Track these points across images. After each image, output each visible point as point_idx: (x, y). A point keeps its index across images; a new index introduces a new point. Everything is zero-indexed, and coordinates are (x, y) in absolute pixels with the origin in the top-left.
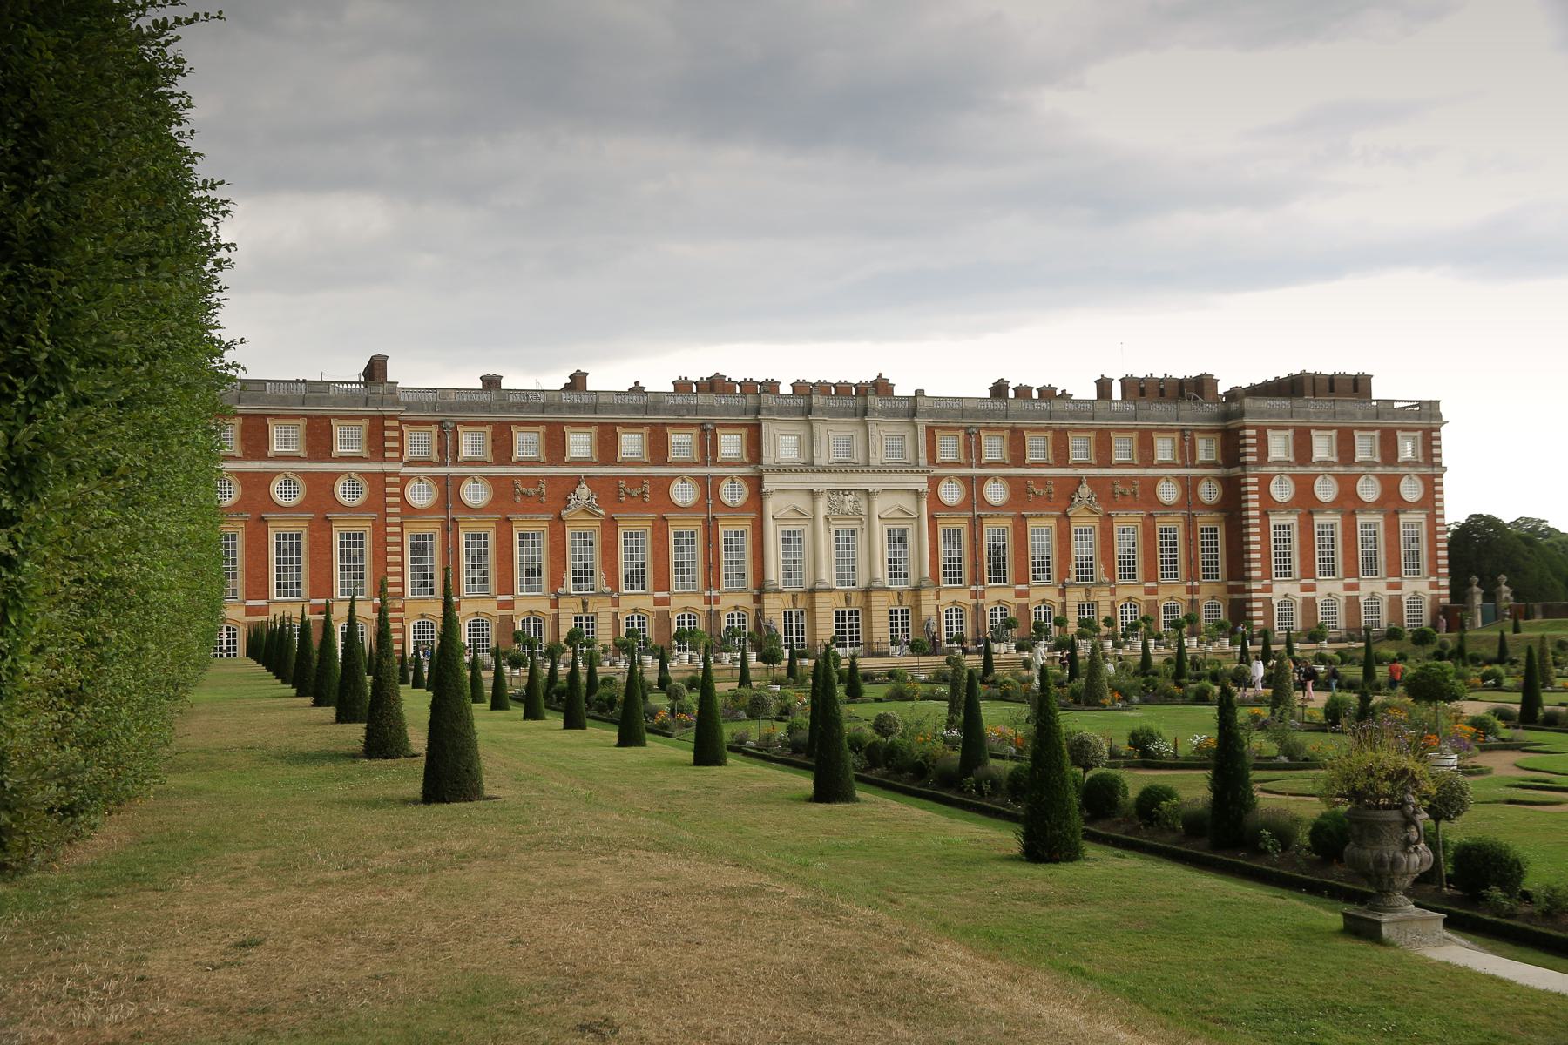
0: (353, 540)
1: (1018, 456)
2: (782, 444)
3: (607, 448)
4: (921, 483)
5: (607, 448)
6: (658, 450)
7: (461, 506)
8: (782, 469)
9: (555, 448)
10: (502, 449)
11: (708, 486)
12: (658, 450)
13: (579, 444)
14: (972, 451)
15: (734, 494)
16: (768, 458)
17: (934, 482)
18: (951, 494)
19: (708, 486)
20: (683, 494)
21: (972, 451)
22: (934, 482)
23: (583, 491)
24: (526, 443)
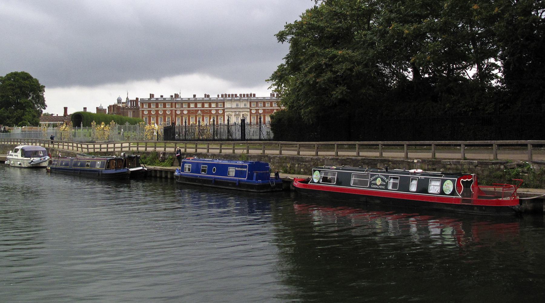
0: (168, 118)
1: (264, 106)
2: (227, 105)
3: (203, 106)
4: (249, 110)
5: (203, 106)
6: (210, 106)
7: (183, 114)
8: (227, 108)
9: (196, 106)
10: (189, 106)
11: (217, 111)
12: (210, 106)
13: (199, 105)
14: (257, 105)
15: (221, 112)
16: (225, 107)
17: (251, 110)
18: (253, 112)
19: (217, 111)
20: (213, 112)
21: (257, 105)
22: (251, 110)
23: (199, 112)
24: (192, 106)
